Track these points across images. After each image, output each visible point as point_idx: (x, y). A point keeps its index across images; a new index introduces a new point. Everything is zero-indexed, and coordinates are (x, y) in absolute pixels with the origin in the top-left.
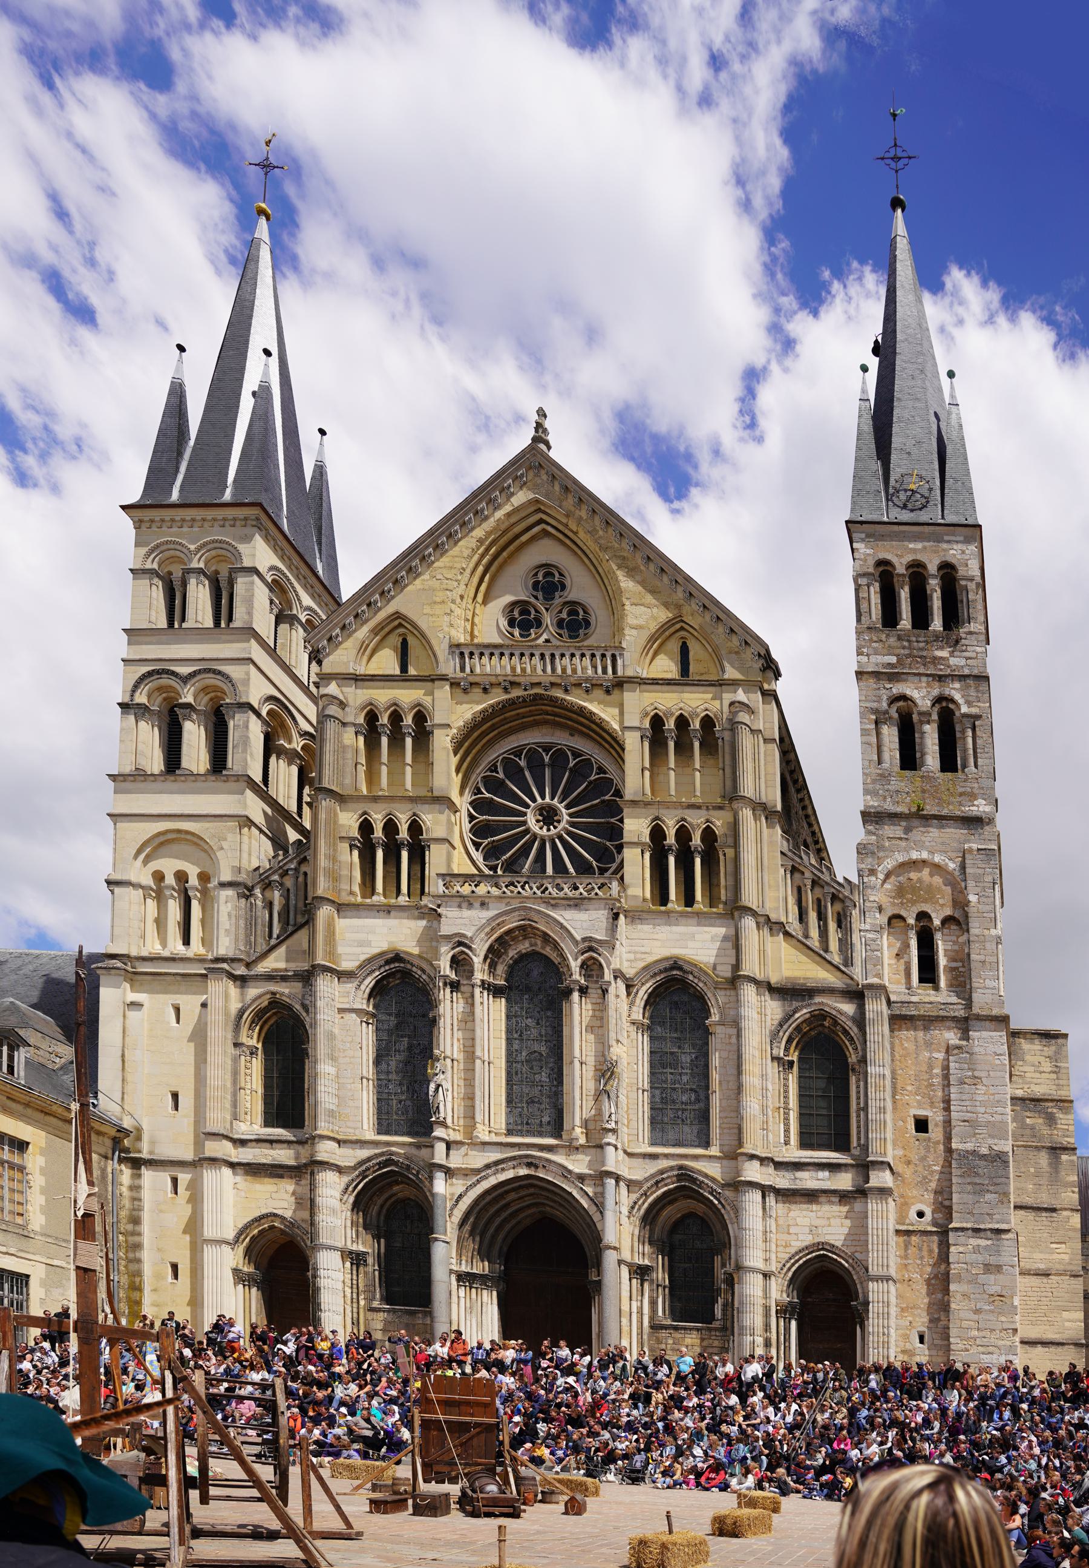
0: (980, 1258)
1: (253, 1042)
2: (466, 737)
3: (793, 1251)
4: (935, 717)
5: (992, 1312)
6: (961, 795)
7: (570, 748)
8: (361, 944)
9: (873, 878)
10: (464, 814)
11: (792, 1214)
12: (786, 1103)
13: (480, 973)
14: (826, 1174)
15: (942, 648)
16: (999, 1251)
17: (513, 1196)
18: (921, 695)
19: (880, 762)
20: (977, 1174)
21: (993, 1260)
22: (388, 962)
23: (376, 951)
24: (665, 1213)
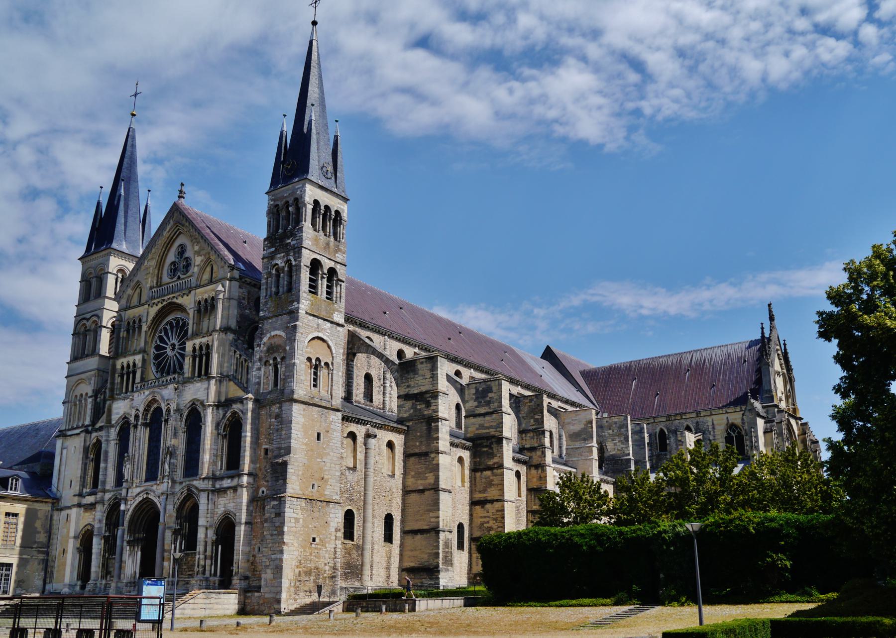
0: (273, 510)
1: (92, 456)
2: (152, 324)
3: (218, 515)
4: (286, 269)
5: (276, 534)
6: (290, 302)
7: (181, 318)
8: (117, 414)
9: (258, 348)
10: (152, 354)
11: (220, 500)
12: (222, 452)
13: (141, 421)
14: (229, 481)
15: (289, 239)
16: (280, 506)
17: (145, 506)
18: (280, 262)
19: (266, 296)
20: (277, 472)
21: (278, 512)
22: (123, 419)
23: (120, 415)
24: (187, 505)
